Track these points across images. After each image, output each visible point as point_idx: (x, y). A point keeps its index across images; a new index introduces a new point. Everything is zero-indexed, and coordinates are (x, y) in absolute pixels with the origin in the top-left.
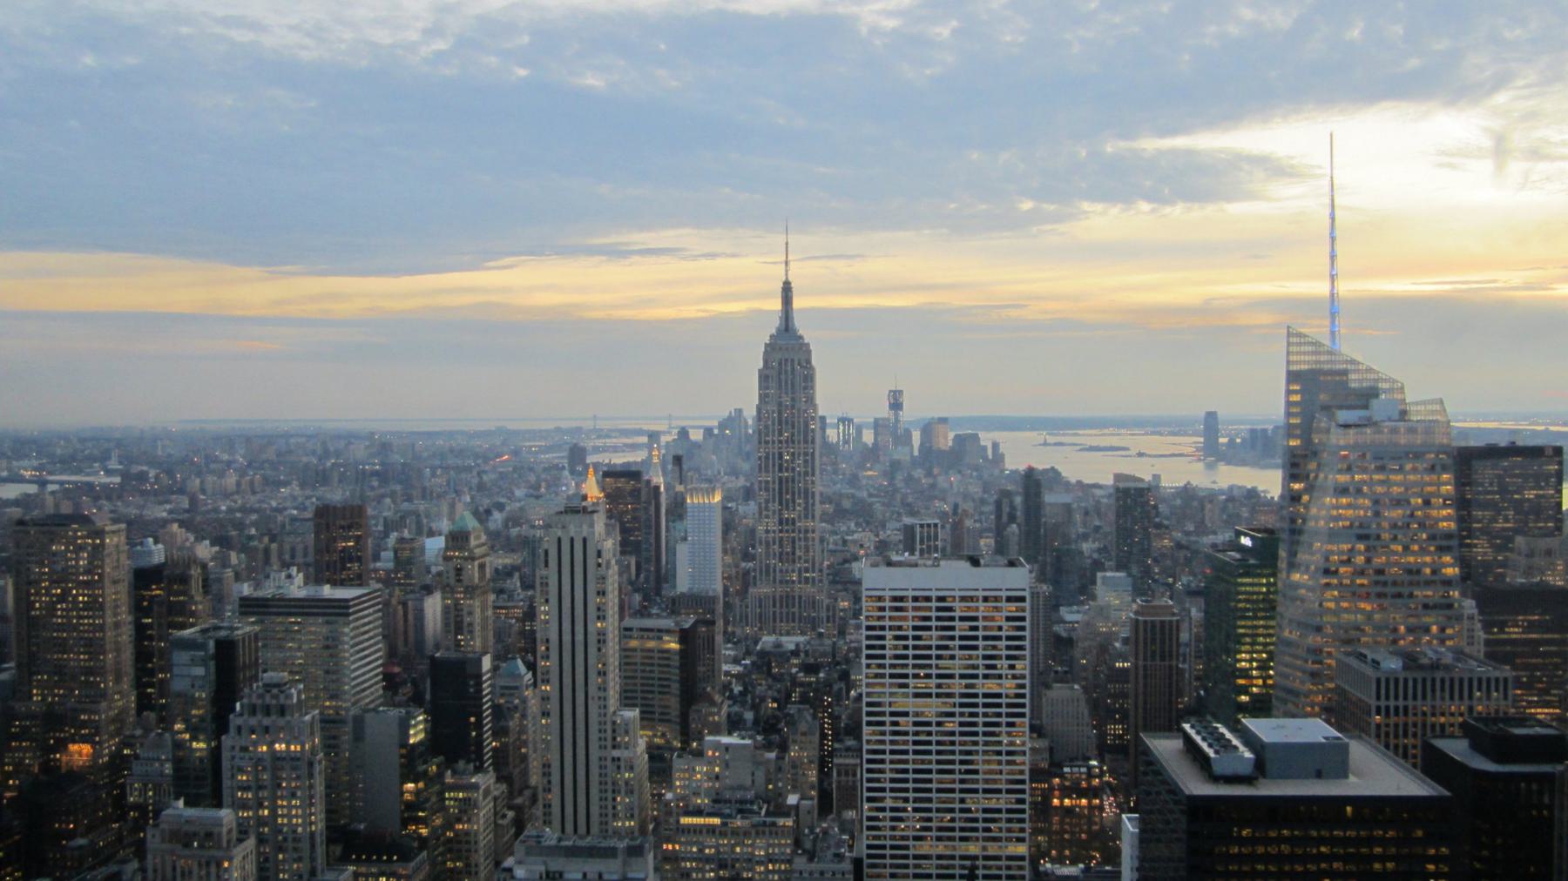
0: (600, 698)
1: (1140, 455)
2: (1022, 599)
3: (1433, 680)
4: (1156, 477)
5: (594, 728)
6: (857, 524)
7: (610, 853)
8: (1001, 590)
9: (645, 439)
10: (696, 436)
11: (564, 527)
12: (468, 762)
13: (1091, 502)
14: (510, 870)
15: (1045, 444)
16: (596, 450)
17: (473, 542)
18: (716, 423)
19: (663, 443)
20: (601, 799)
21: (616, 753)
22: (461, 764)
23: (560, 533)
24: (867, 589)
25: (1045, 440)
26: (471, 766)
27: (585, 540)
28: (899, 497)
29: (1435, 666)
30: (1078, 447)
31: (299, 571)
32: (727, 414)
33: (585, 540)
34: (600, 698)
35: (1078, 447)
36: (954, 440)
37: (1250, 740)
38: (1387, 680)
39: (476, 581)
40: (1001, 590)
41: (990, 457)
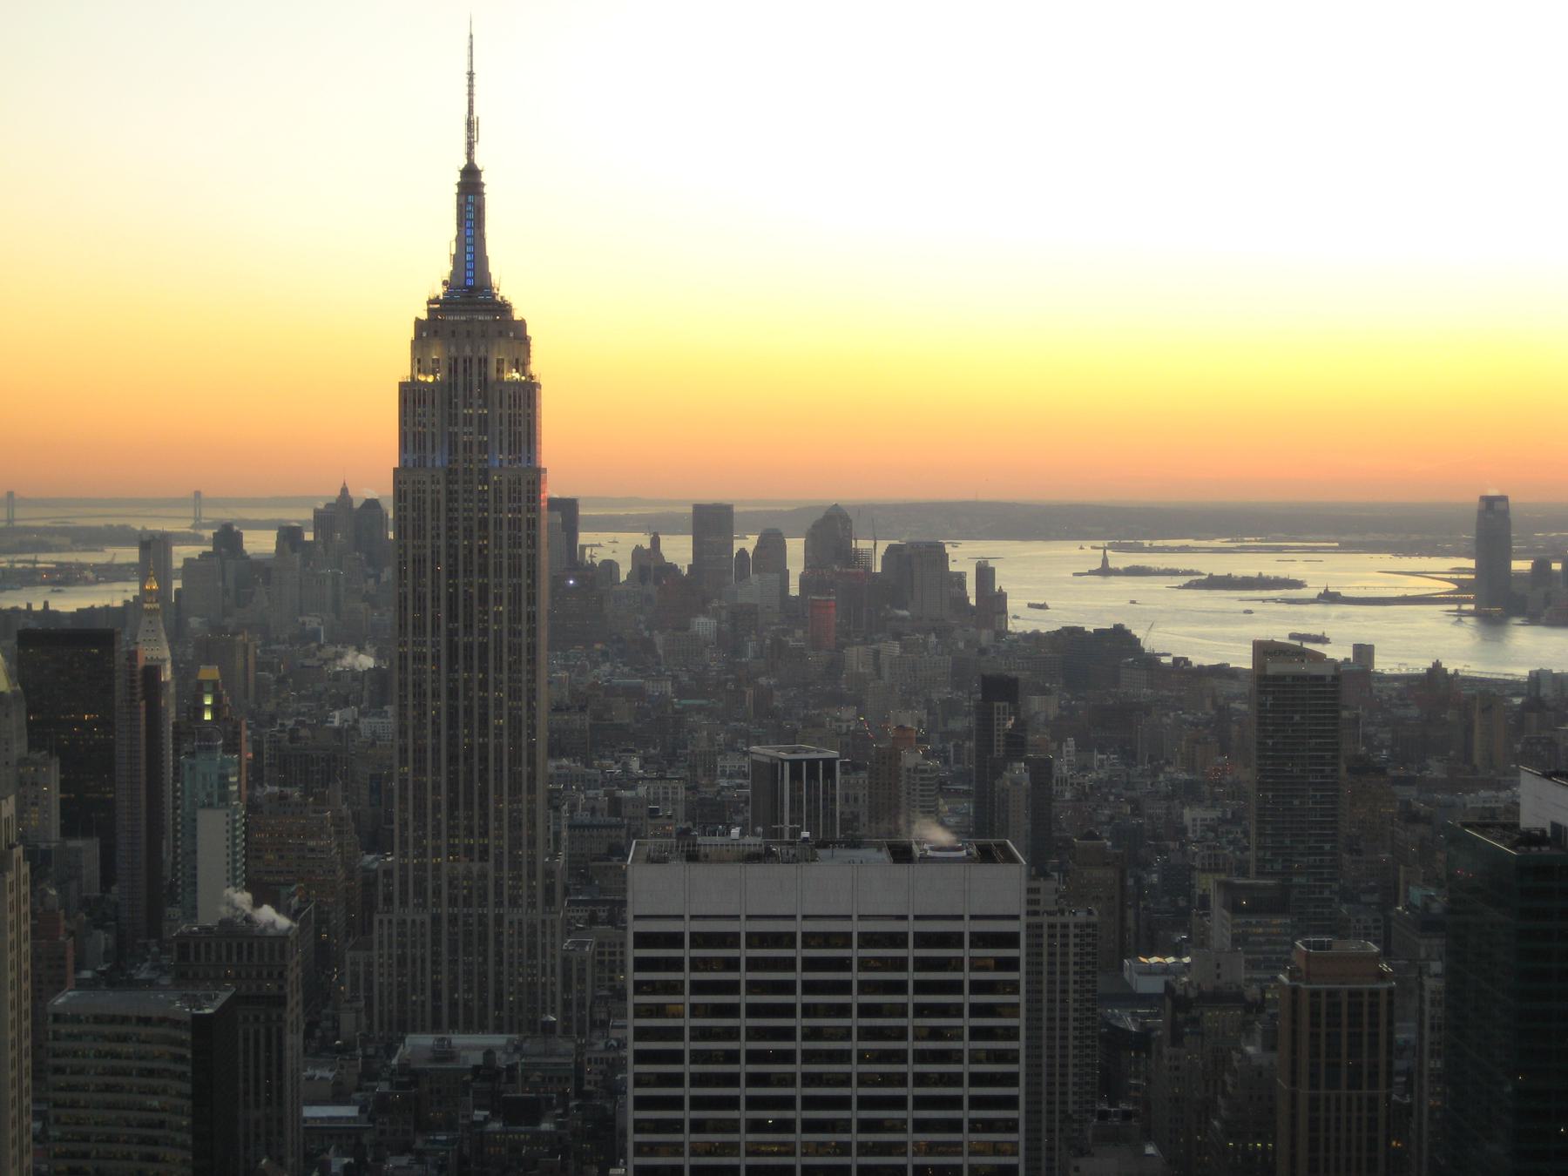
1: (1329, 598)
4: (1364, 652)
6: (645, 761)
9: (131, 555)
10: (259, 543)
13: (1208, 703)
15: (1105, 571)
18: (308, 515)
19: (177, 563)
25: (1105, 561)
28: (750, 692)
30: (1186, 580)
32: (338, 493)
35: (1186, 580)
36: (884, 558)
41: (973, 601)
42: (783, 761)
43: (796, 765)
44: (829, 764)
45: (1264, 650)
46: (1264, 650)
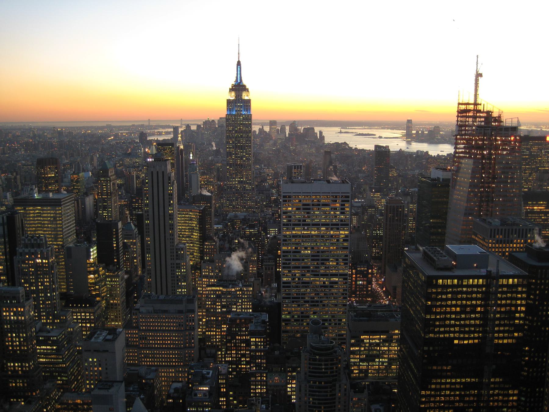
0: (171, 239)
2: (348, 197)
3: (512, 229)
5: (168, 251)
7: (180, 302)
8: (339, 193)
11: (154, 167)
12: (114, 265)
14: (138, 309)
16: (153, 134)
17: (110, 174)
20: (172, 280)
21: (178, 262)
22: (111, 267)
23: (152, 170)
24: (283, 193)
26: (115, 267)
27: (163, 172)
29: (514, 224)
31: (35, 187)
33: (163, 172)
34: (171, 239)
37: (450, 253)
38: (495, 230)
39: (112, 190)
40: (339, 193)
42: (293, 166)
43: (295, 166)
44: (301, 166)
45: (377, 147)
46: (377, 147)
